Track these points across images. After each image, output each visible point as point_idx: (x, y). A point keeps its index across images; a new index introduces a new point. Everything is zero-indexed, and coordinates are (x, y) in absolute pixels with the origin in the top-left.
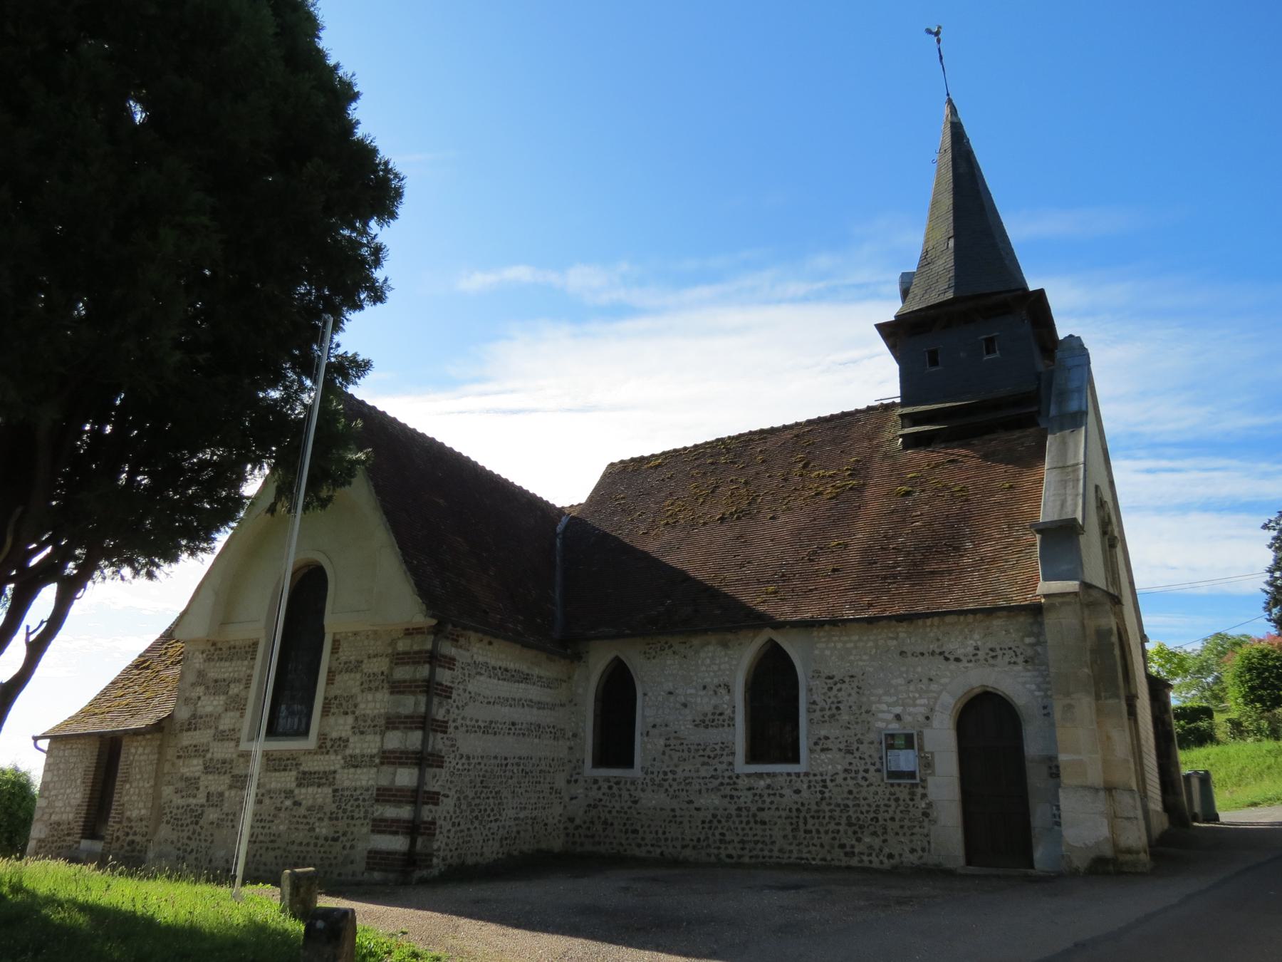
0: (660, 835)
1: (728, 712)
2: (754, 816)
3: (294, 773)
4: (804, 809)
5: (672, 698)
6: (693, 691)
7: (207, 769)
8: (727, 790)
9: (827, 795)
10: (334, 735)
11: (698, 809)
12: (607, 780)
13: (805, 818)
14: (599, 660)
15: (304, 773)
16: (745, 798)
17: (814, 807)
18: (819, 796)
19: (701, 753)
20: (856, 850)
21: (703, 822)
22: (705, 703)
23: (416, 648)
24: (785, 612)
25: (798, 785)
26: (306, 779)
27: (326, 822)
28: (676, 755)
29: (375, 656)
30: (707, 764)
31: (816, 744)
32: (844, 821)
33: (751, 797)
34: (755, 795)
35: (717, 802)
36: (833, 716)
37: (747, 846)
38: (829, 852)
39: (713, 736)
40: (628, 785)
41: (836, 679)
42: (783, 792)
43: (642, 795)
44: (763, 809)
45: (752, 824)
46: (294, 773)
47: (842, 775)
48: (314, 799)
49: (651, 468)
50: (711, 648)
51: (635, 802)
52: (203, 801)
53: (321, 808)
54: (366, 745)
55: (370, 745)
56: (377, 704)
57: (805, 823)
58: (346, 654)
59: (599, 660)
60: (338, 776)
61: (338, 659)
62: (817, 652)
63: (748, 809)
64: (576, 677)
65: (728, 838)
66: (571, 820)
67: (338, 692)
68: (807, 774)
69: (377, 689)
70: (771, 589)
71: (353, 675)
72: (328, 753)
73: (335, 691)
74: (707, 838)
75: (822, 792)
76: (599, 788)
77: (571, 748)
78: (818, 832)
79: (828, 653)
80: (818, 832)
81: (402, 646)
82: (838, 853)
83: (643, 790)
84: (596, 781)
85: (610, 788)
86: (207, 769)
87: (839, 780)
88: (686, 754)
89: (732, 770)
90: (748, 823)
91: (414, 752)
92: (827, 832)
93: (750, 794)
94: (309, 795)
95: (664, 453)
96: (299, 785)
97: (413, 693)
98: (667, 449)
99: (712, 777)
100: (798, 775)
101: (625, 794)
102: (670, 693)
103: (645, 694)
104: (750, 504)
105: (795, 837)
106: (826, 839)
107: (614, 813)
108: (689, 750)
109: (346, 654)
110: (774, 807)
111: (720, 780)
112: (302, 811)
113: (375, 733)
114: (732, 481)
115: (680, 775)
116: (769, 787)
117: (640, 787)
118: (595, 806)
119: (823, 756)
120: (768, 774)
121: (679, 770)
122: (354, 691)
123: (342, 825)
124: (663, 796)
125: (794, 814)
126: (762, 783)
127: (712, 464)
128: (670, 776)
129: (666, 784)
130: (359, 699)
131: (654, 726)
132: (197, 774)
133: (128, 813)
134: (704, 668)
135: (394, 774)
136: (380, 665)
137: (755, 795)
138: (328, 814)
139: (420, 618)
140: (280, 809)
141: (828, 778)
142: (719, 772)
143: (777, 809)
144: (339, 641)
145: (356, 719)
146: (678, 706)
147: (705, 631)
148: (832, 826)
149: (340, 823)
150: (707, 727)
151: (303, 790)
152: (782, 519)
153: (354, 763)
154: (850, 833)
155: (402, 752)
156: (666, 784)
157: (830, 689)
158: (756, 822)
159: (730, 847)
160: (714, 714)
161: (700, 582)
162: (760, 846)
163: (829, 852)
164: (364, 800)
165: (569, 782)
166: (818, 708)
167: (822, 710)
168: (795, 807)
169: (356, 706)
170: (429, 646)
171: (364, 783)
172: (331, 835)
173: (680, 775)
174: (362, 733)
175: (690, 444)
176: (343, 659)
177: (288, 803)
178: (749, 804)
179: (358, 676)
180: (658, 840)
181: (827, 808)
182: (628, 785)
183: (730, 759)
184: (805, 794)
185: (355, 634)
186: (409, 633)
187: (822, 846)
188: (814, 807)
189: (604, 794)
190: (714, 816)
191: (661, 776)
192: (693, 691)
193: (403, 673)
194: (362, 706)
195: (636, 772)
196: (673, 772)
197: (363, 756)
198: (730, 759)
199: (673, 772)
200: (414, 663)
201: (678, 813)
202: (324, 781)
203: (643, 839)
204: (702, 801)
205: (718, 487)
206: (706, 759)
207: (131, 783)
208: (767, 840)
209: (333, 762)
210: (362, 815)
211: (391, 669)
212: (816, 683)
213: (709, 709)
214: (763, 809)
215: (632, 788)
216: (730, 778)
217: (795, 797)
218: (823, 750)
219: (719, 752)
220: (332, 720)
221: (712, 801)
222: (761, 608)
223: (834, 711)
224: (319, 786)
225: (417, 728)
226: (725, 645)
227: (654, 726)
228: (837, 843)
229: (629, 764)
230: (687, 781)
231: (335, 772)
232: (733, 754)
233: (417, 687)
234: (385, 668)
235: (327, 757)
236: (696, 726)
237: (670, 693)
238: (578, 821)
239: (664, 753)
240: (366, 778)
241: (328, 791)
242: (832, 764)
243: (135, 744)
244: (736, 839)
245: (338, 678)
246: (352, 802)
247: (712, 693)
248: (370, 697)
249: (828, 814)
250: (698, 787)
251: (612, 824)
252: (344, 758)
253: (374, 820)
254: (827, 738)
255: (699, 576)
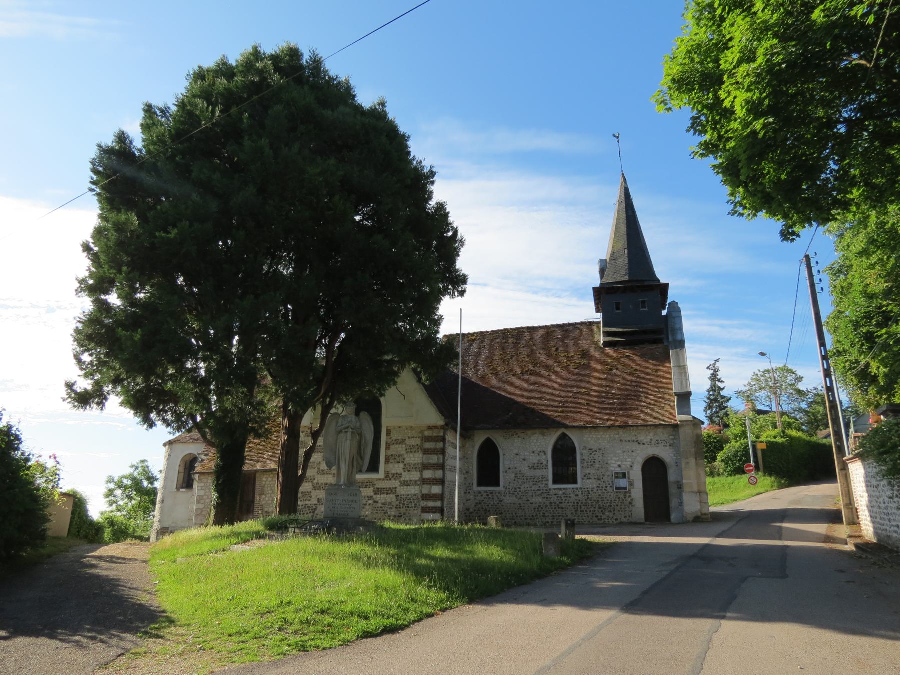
0: (514, 514)
1: (545, 463)
2: (558, 506)
3: (372, 489)
4: (580, 503)
5: (518, 457)
6: (528, 454)
7: (315, 488)
8: (546, 496)
9: (590, 497)
10: (393, 472)
11: (532, 504)
12: (486, 492)
13: (581, 506)
14: (480, 439)
15: (378, 489)
16: (554, 499)
17: (584, 502)
18: (586, 497)
19: (533, 480)
20: (603, 518)
21: (535, 509)
22: (534, 459)
23: (435, 435)
24: (570, 421)
25: (577, 493)
26: (378, 491)
27: (394, 509)
28: (520, 481)
29: (413, 438)
30: (536, 485)
31: (585, 476)
32: (597, 507)
33: (556, 498)
34: (558, 497)
35: (541, 500)
36: (592, 465)
37: (556, 518)
38: (591, 519)
39: (539, 473)
40: (497, 494)
41: (594, 450)
42: (571, 496)
43: (504, 498)
44: (562, 503)
45: (557, 509)
46: (372, 489)
47: (596, 489)
48: (386, 500)
49: (470, 341)
50: (536, 436)
51: (501, 501)
52: (316, 502)
53: (390, 504)
54: (412, 476)
55: (415, 476)
56: (417, 458)
57: (581, 508)
58: (395, 436)
59: (480, 439)
60: (398, 490)
61: (391, 438)
62: (585, 439)
63: (555, 503)
64: (467, 446)
65: (547, 515)
66: (468, 510)
67: (394, 453)
68: (581, 489)
69: (415, 452)
70: (560, 410)
71: (401, 446)
72: (391, 480)
73: (390, 453)
74: (537, 515)
75: (588, 496)
76: (482, 496)
77: (465, 478)
78: (586, 511)
79: (590, 439)
80: (586, 511)
81: (427, 434)
82: (595, 519)
83: (505, 496)
84: (480, 493)
85: (488, 495)
86: (315, 488)
87: (595, 490)
88: (525, 481)
89: (548, 487)
90: (555, 509)
91: (440, 479)
92: (590, 511)
93: (556, 497)
94: (381, 498)
95: (475, 333)
96: (376, 494)
97: (437, 454)
98: (477, 331)
99: (538, 490)
100: (577, 489)
101: (496, 498)
102: (517, 455)
103: (504, 455)
104: (534, 367)
105: (576, 514)
106: (590, 514)
107: (490, 506)
108: (527, 479)
109: (395, 436)
110: (567, 502)
111: (542, 491)
112: (380, 505)
113: (417, 471)
114: (520, 354)
115: (523, 489)
116: (564, 494)
117: (503, 495)
118: (480, 504)
119: (588, 481)
120: (564, 489)
121: (522, 488)
122: (402, 453)
123: (403, 510)
124: (515, 498)
125: (576, 504)
126: (561, 492)
127: (506, 343)
128: (518, 490)
129: (516, 494)
130: (406, 456)
131: (510, 469)
132: (309, 491)
133: (266, 510)
134: (533, 444)
135: (431, 489)
136: (418, 442)
137: (558, 497)
138: (395, 506)
139: (441, 422)
140: (366, 505)
141: (590, 490)
142: (541, 488)
143: (568, 503)
144: (390, 430)
145: (405, 465)
146: (521, 460)
147: (535, 429)
148: (592, 509)
149: (402, 510)
150: (535, 469)
151: (379, 496)
152: (554, 377)
153: (406, 484)
154: (600, 511)
155: (434, 479)
156: (516, 494)
157: (591, 454)
158: (559, 508)
159: (547, 518)
160: (538, 464)
161: (523, 405)
162: (561, 517)
163: (591, 519)
164: (414, 500)
165: (465, 493)
166: (585, 462)
167: (588, 463)
168: (576, 502)
169: (404, 459)
170: (442, 434)
171: (413, 493)
172: (398, 514)
173: (523, 489)
174: (409, 471)
175: (489, 330)
176: (394, 438)
177: (370, 502)
178: (555, 501)
179: (404, 446)
180: (513, 517)
181: (590, 502)
182: (497, 494)
183: (546, 483)
184: (580, 496)
185: (400, 427)
186: (430, 428)
187: (588, 517)
188: (584, 502)
189: (485, 498)
190: (540, 506)
191: (514, 490)
192: (528, 454)
193: (428, 445)
194: (408, 459)
195: (501, 488)
196: (519, 488)
197: (411, 481)
198: (546, 483)
199: (519, 488)
200: (435, 441)
201: (522, 505)
202: (390, 492)
203: (506, 517)
204: (534, 500)
205: (514, 356)
206: (535, 483)
207: (266, 495)
208: (564, 515)
209: (395, 484)
210: (413, 506)
211: (422, 444)
212: (585, 452)
213: (536, 462)
214: (562, 503)
215: (499, 495)
216: (546, 490)
217: (576, 498)
218: (588, 479)
219: (541, 480)
220: (391, 466)
221: (538, 500)
222: (559, 419)
223: (592, 463)
224: (387, 494)
225: (440, 469)
226: (543, 435)
227: (510, 469)
228: (594, 516)
229: (497, 484)
230: (526, 492)
231: (396, 488)
232: (548, 480)
233: (439, 452)
234: (419, 444)
235: (391, 482)
236: (530, 469)
237: (517, 455)
238: (471, 510)
239: (515, 480)
240: (414, 490)
241: (393, 496)
242: (591, 484)
243: (266, 476)
244: (550, 515)
245: (392, 447)
246: (407, 501)
247: (537, 455)
248: (412, 456)
249: (590, 504)
250: (531, 494)
251: (489, 511)
252: (401, 482)
253: (423, 508)
254: (590, 474)
255: (523, 401)
